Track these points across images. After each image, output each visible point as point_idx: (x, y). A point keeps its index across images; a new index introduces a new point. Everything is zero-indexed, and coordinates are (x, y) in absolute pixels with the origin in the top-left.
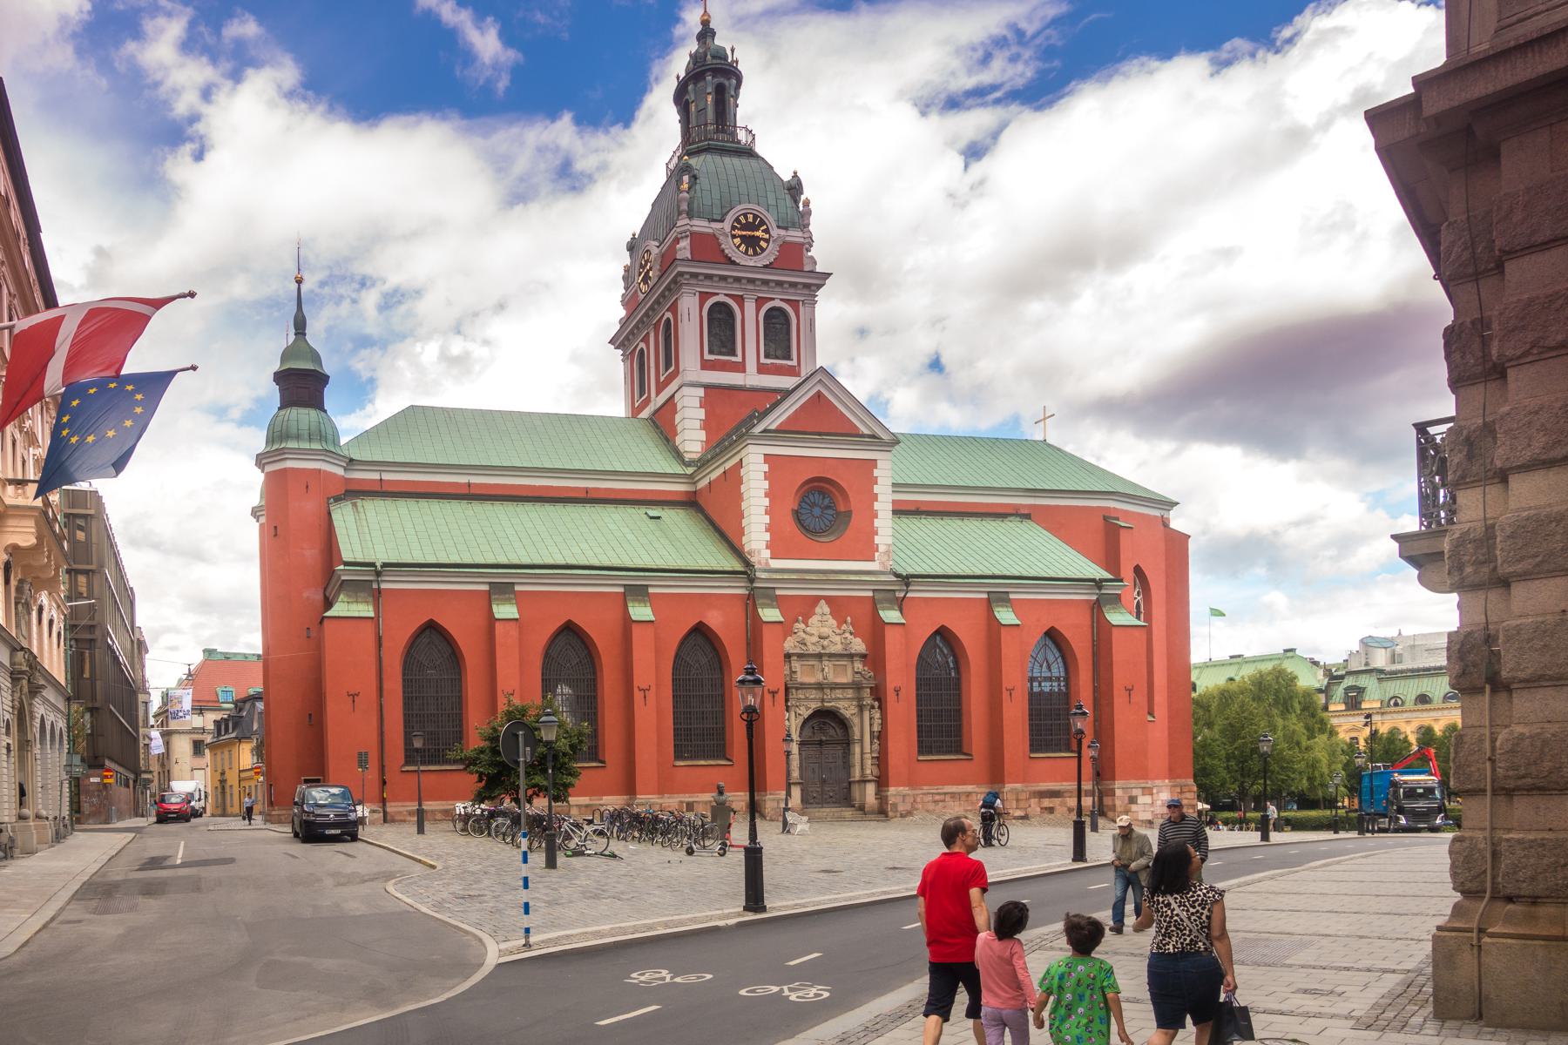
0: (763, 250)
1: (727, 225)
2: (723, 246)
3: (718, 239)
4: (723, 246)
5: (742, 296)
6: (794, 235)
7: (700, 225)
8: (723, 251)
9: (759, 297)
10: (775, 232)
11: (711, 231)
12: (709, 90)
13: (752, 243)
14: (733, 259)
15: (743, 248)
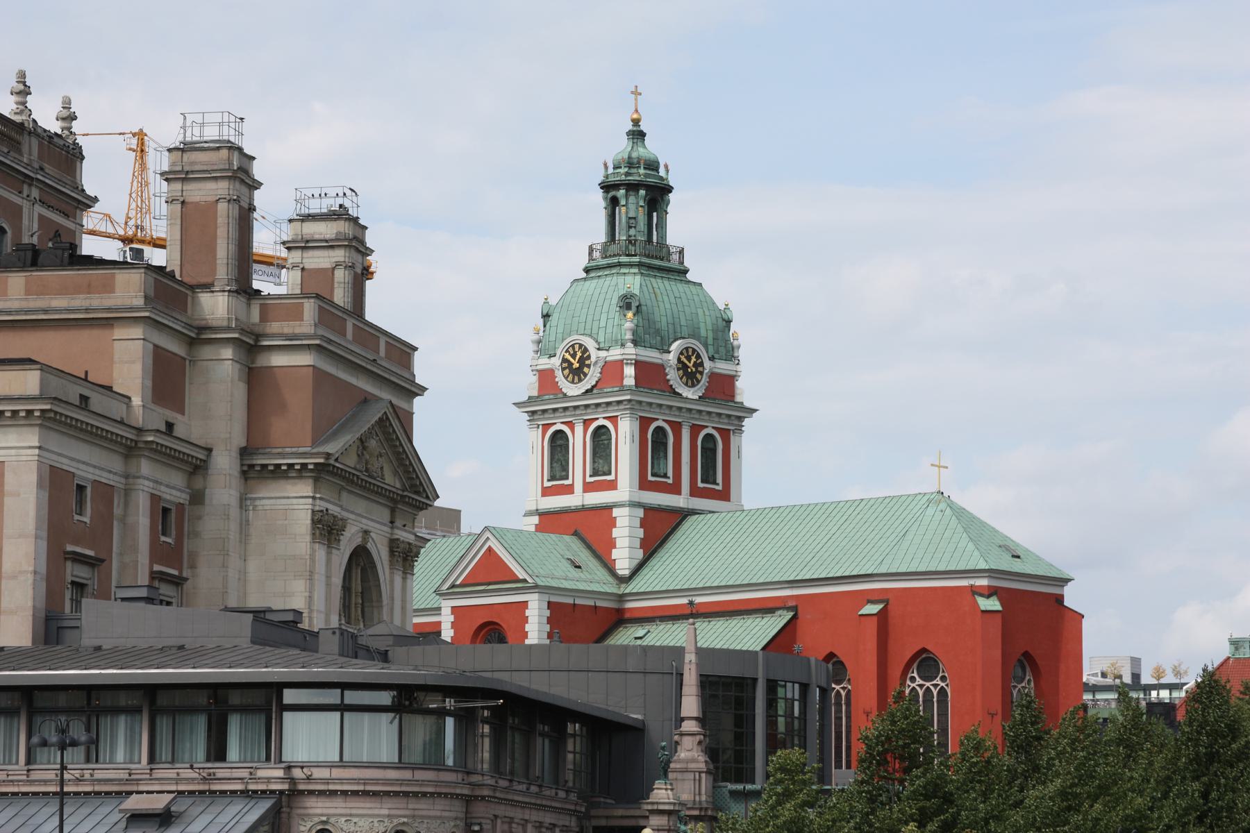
0: (699, 382)
1: (672, 358)
2: (668, 377)
3: (665, 369)
4: (668, 377)
5: (680, 423)
6: (722, 367)
7: (651, 355)
8: (671, 386)
9: (693, 424)
10: (708, 364)
11: (660, 361)
12: (642, 203)
13: (691, 378)
14: (677, 390)
15: (684, 379)
